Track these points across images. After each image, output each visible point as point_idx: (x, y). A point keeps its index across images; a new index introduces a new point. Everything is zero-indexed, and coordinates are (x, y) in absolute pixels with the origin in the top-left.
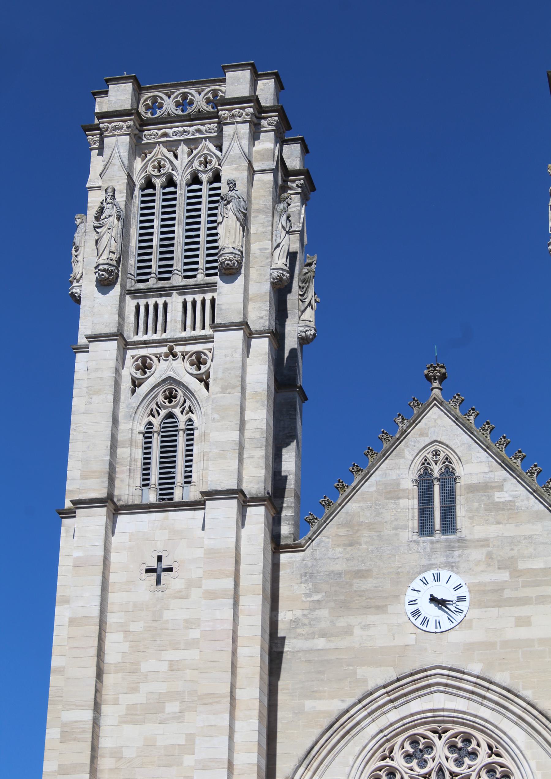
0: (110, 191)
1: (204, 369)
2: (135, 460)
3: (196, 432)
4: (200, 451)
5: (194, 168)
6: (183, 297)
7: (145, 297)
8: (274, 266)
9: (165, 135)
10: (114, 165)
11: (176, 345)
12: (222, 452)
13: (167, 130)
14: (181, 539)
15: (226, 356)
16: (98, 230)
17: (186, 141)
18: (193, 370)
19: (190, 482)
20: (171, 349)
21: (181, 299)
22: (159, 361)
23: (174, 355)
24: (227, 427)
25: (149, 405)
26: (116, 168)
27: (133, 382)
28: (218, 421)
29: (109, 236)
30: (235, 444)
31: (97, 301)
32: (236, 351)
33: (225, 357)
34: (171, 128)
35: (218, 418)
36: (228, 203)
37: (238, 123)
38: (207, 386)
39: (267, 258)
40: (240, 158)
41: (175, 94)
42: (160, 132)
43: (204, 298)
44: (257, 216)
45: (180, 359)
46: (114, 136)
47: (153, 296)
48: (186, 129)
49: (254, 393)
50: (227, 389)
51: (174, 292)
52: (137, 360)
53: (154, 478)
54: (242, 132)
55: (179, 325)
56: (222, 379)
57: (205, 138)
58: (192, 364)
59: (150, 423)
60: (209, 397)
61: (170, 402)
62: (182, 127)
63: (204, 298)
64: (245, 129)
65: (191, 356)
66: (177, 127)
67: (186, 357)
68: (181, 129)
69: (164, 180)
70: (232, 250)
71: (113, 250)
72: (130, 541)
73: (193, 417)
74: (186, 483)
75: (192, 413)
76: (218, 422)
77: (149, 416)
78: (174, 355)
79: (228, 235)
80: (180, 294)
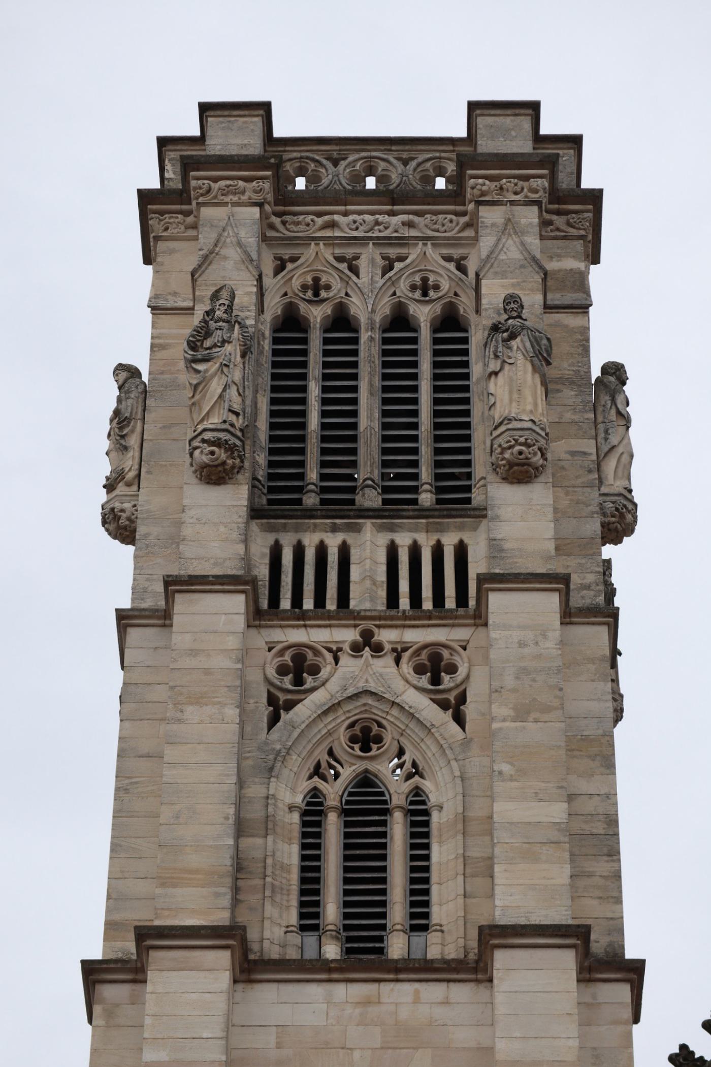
0: (224, 294)
1: (447, 681)
2: (285, 868)
3: (435, 817)
4: (453, 856)
5: (398, 294)
6: (389, 536)
7: (297, 529)
8: (604, 490)
9: (333, 225)
10: (225, 258)
11: (378, 627)
12: (527, 845)
13: (336, 217)
14: (416, 1048)
15: (522, 644)
16: (200, 367)
17: (381, 242)
18: (424, 681)
19: (425, 928)
20: (367, 635)
21: (383, 540)
22: (337, 660)
23: (377, 649)
24: (536, 793)
25: (311, 752)
26: (229, 264)
27: (272, 700)
28: (512, 779)
29: (224, 380)
30: (559, 830)
31: (192, 513)
32: (545, 636)
33: (520, 647)
34: (346, 214)
35: (513, 773)
36: (513, 336)
37: (512, 203)
38: (459, 719)
39: (590, 471)
40: (522, 266)
41: (351, 158)
42: (320, 221)
43: (439, 542)
44: (558, 391)
45: (389, 660)
46: (225, 204)
47: (315, 529)
48: (380, 218)
49: (582, 739)
50: (528, 713)
51: (368, 524)
52: (281, 653)
53: (332, 911)
54: (523, 221)
55: (382, 593)
56: (514, 690)
57: (425, 239)
58: (419, 670)
59: (315, 792)
60: (466, 743)
61: (366, 748)
62: (372, 213)
63: (439, 542)
64: (530, 217)
65: (417, 653)
66: (360, 213)
67: (406, 656)
68: (368, 218)
69: (329, 312)
70: (529, 425)
71: (237, 407)
72: (279, 1046)
73: (427, 785)
74: (414, 928)
75: (422, 776)
76: (511, 780)
77: (310, 777)
78: (377, 649)
79: (515, 396)
80: (381, 528)
